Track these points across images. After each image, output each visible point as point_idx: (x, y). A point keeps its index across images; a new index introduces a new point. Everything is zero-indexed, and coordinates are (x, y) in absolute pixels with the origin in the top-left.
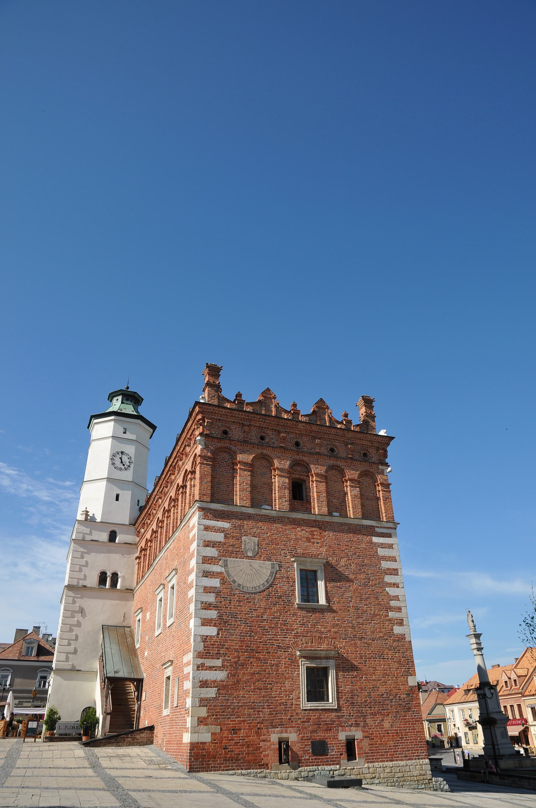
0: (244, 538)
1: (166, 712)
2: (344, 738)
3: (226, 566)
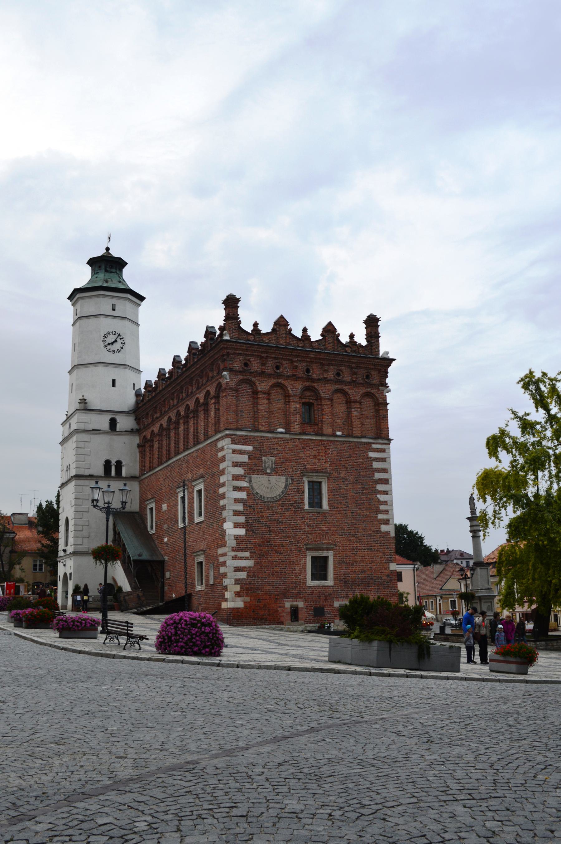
0: (263, 458)
1: (199, 588)
2: (338, 606)
3: (250, 481)
